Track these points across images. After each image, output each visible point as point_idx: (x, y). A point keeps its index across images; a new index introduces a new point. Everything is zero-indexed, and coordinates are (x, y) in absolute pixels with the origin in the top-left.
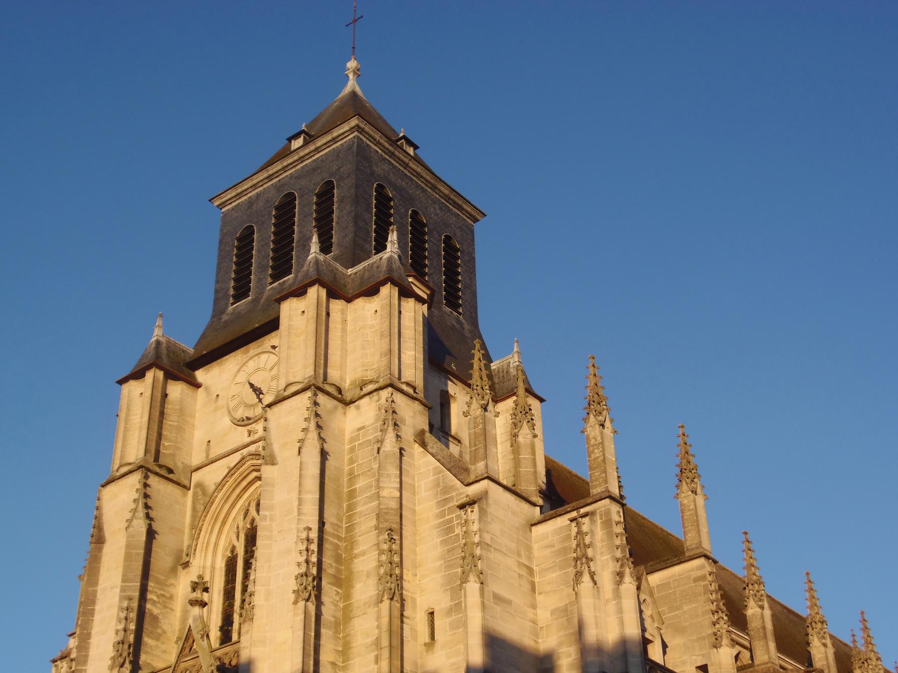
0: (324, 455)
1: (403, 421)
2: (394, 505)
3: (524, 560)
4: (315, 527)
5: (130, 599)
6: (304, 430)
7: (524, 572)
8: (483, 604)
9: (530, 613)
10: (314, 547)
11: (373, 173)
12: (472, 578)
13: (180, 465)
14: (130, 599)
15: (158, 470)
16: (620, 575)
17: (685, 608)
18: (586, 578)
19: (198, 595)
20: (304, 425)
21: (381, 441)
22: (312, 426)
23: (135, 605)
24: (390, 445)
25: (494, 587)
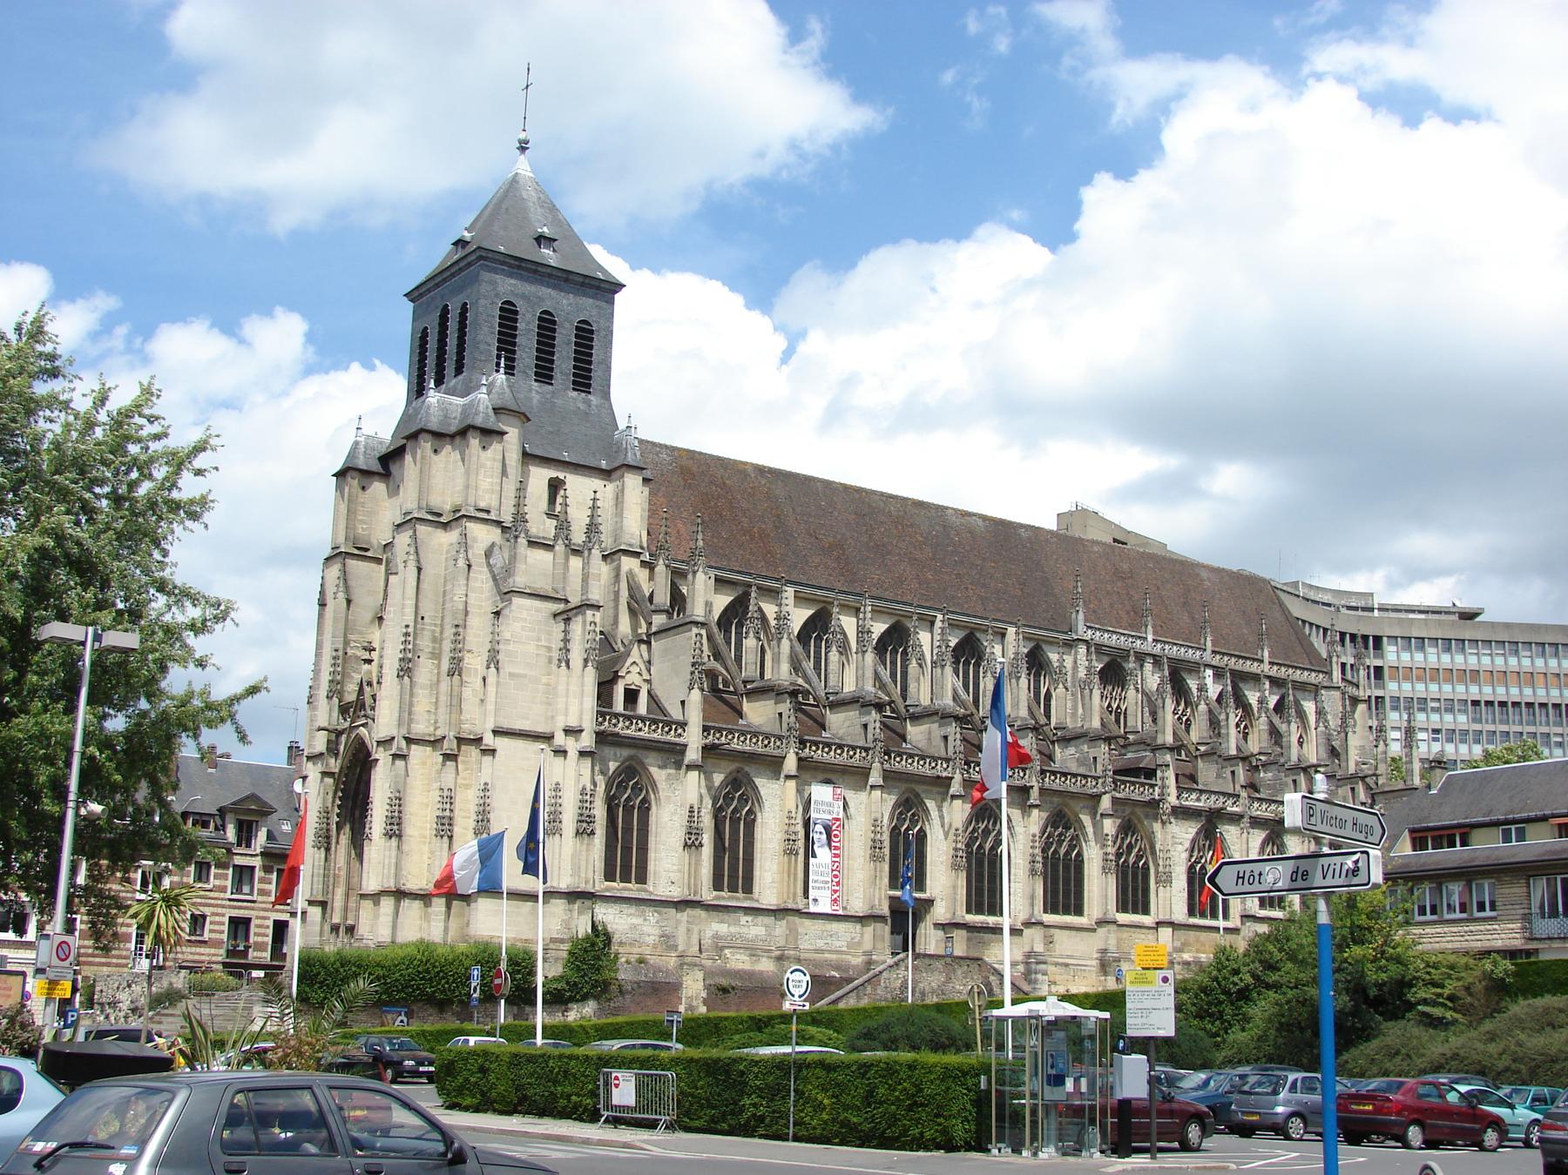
0: (419, 569)
1: (475, 540)
2: (461, 607)
3: (543, 643)
4: (412, 624)
5: (336, 650)
6: (407, 553)
7: (543, 652)
8: (498, 683)
9: (544, 679)
10: (411, 638)
11: (497, 295)
12: (492, 665)
13: (375, 542)
14: (336, 650)
15: (356, 552)
16: (586, 661)
17: (681, 658)
18: (563, 664)
19: (366, 656)
20: (408, 549)
21: (456, 560)
22: (412, 550)
23: (340, 653)
24: (461, 563)
25: (506, 668)
